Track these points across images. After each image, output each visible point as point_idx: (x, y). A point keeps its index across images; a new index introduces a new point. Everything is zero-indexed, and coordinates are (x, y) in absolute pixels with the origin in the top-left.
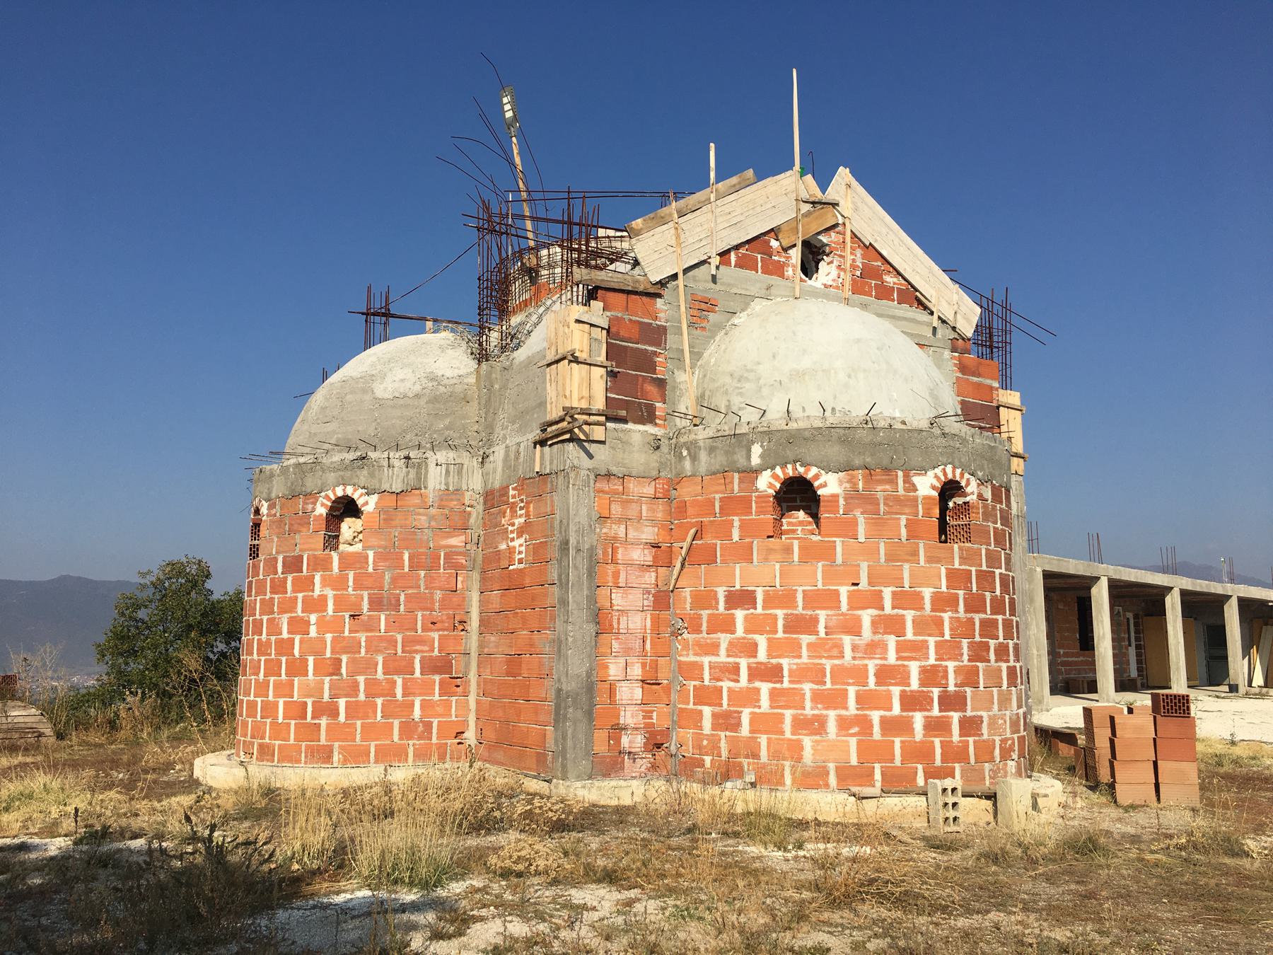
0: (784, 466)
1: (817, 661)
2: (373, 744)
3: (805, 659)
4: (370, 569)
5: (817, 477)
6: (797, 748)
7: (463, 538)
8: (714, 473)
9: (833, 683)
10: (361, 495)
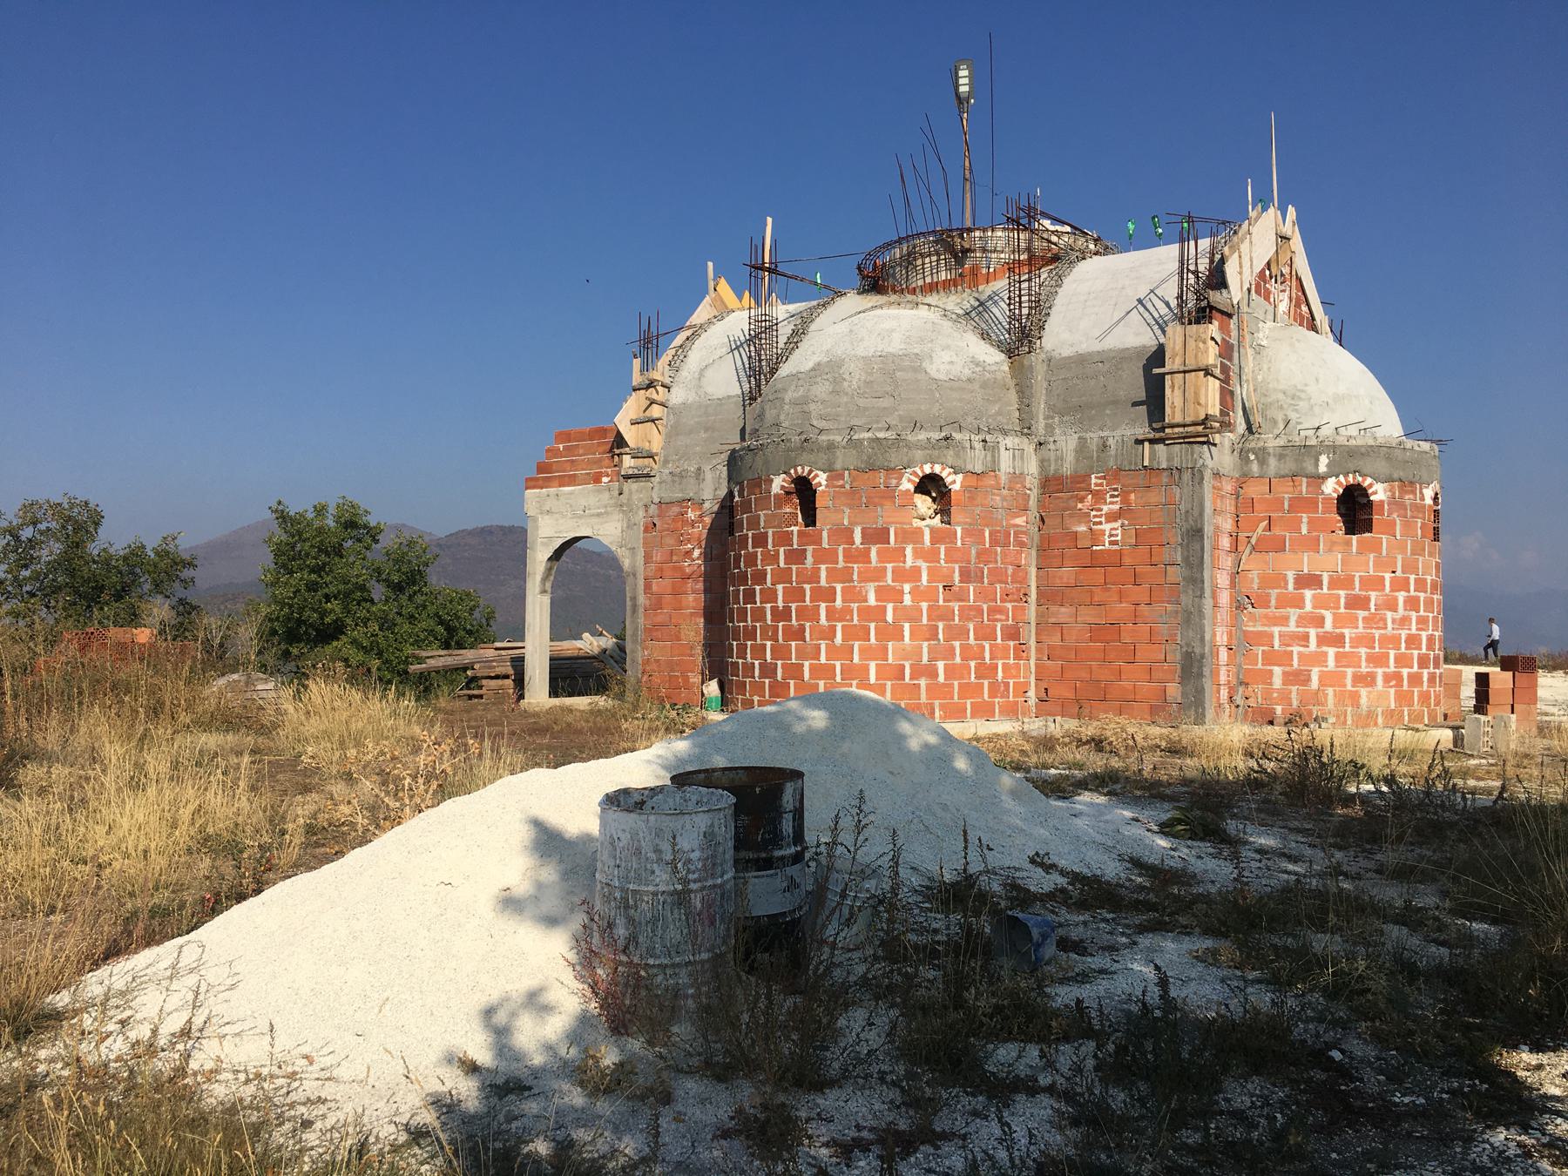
0: (1346, 476)
1: (1369, 631)
2: (969, 702)
3: (1361, 630)
4: (959, 543)
5: (1371, 485)
6: (1355, 697)
7: (1024, 518)
8: (1284, 477)
9: (1380, 648)
10: (950, 474)
